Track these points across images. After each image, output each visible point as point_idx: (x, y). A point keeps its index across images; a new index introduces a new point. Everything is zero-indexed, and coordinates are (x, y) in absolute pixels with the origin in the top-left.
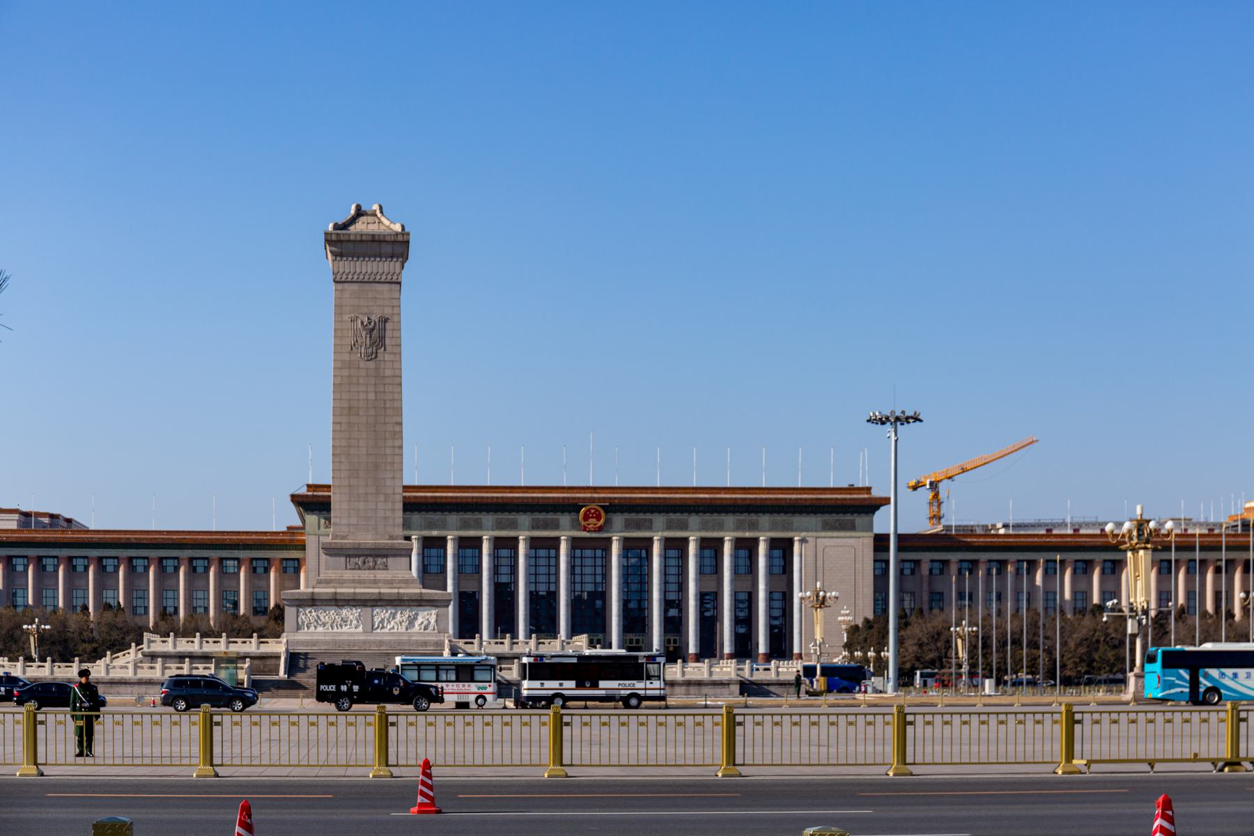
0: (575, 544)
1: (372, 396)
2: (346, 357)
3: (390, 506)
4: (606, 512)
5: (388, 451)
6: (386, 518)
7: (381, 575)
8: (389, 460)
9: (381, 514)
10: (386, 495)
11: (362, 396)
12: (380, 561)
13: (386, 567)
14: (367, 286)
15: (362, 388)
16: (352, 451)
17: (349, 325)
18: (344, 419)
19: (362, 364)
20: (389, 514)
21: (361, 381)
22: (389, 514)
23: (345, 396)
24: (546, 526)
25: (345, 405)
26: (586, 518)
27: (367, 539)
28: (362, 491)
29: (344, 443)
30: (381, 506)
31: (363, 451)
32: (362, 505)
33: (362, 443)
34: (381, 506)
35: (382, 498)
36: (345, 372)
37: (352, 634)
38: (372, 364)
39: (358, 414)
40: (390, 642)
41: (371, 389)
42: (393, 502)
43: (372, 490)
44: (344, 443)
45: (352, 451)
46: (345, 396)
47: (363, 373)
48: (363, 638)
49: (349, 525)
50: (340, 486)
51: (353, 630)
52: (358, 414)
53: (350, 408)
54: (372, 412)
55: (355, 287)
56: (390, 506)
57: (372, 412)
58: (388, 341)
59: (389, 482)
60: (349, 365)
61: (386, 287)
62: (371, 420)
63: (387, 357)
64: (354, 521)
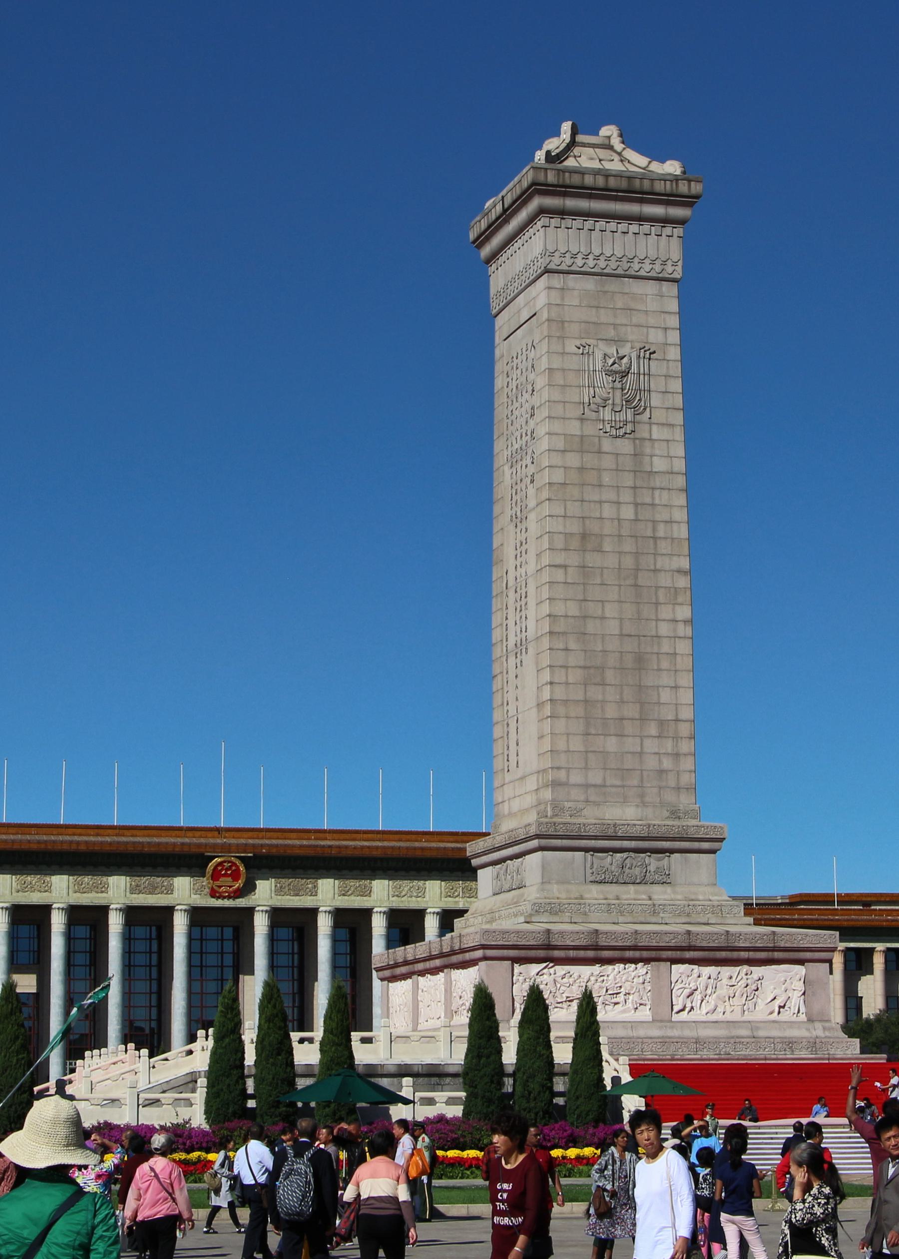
0: (197, 915)
1: (628, 513)
2: (574, 428)
3: (669, 746)
4: (246, 868)
5: (664, 629)
6: (661, 772)
7: (661, 894)
8: (666, 647)
9: (651, 763)
10: (662, 723)
11: (608, 511)
12: (653, 862)
13: (665, 880)
14: (613, 285)
15: (611, 495)
16: (591, 627)
17: (574, 363)
18: (574, 559)
19: (607, 445)
20: (667, 763)
21: (607, 479)
22: (667, 763)
23: (574, 509)
24: (152, 890)
25: (574, 527)
26: (216, 876)
27: (627, 815)
28: (611, 712)
29: (573, 609)
30: (650, 746)
31: (613, 627)
32: (611, 744)
33: (610, 611)
34: (650, 746)
35: (653, 730)
36: (573, 460)
37: (634, 1024)
38: (625, 446)
39: (599, 550)
40: (716, 1040)
41: (626, 496)
42: (676, 738)
43: (631, 711)
44: (573, 609)
45: (591, 627)
46: (574, 509)
47: (608, 462)
48: (655, 1032)
49: (587, 786)
50: (566, 702)
51: (630, 1016)
52: (599, 550)
53: (584, 536)
54: (628, 546)
55: (589, 284)
56: (669, 746)
57: (628, 546)
58: (656, 400)
59: (666, 696)
60: (581, 445)
61: (651, 288)
62: (628, 562)
63: (656, 433)
64: (595, 777)
